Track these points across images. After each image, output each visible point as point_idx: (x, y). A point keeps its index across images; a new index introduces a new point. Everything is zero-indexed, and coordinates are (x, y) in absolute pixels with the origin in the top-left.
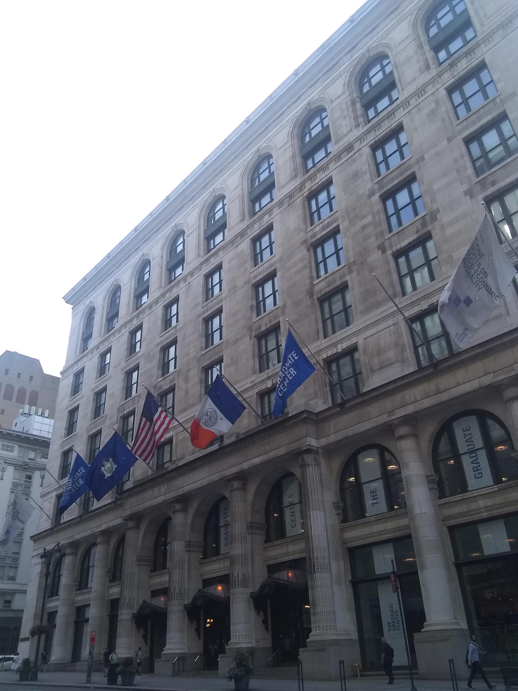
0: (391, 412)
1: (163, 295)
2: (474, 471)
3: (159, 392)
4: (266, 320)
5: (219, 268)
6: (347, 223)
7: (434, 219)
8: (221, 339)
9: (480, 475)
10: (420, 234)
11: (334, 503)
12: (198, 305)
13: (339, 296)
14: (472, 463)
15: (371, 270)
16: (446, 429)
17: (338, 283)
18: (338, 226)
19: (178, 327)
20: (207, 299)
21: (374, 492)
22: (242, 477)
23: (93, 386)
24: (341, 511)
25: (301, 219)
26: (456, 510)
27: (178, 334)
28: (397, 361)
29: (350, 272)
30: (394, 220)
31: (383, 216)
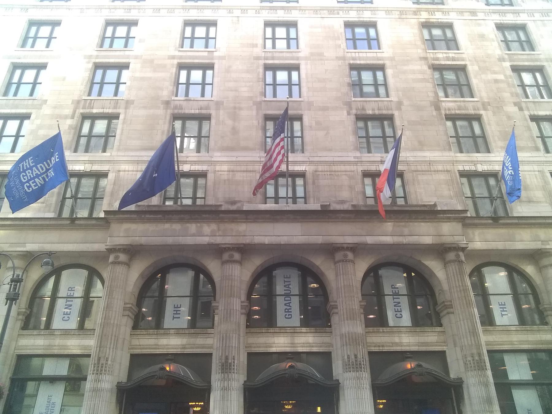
2: (285, 312)
9: (290, 316)
14: (285, 305)
21: (177, 309)
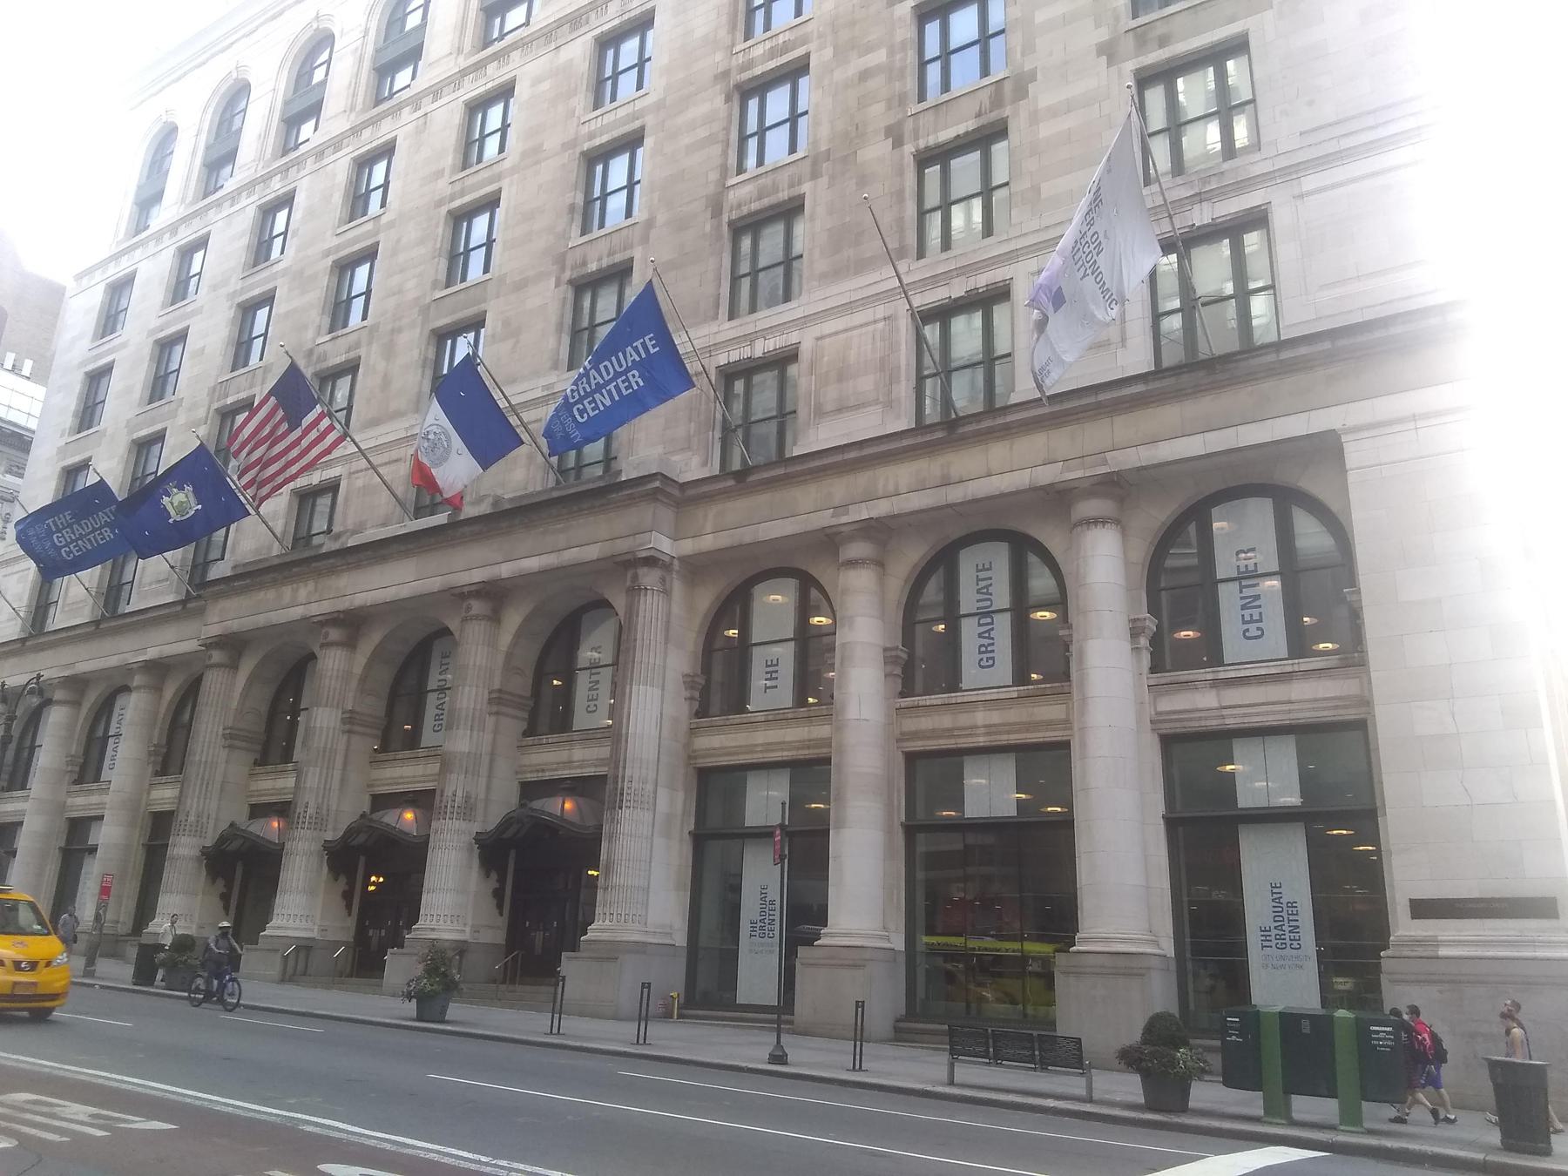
0: (842, 508)
1: (355, 131)
3: (318, 367)
4: (603, 247)
5: (505, 92)
6: (828, 52)
7: (1021, 92)
8: (486, 270)
10: (983, 121)
11: (687, 675)
12: (439, 174)
13: (779, 228)
14: (980, 635)
15: (863, 181)
16: (944, 561)
17: (783, 195)
18: (808, 55)
19: (384, 219)
20: (465, 165)
21: (772, 667)
22: (495, 594)
23: (155, 323)
24: (697, 694)
25: (724, 19)
26: (925, 723)
27: (381, 237)
28: (876, 402)
29: (815, 175)
30: (934, 72)
31: (911, 57)
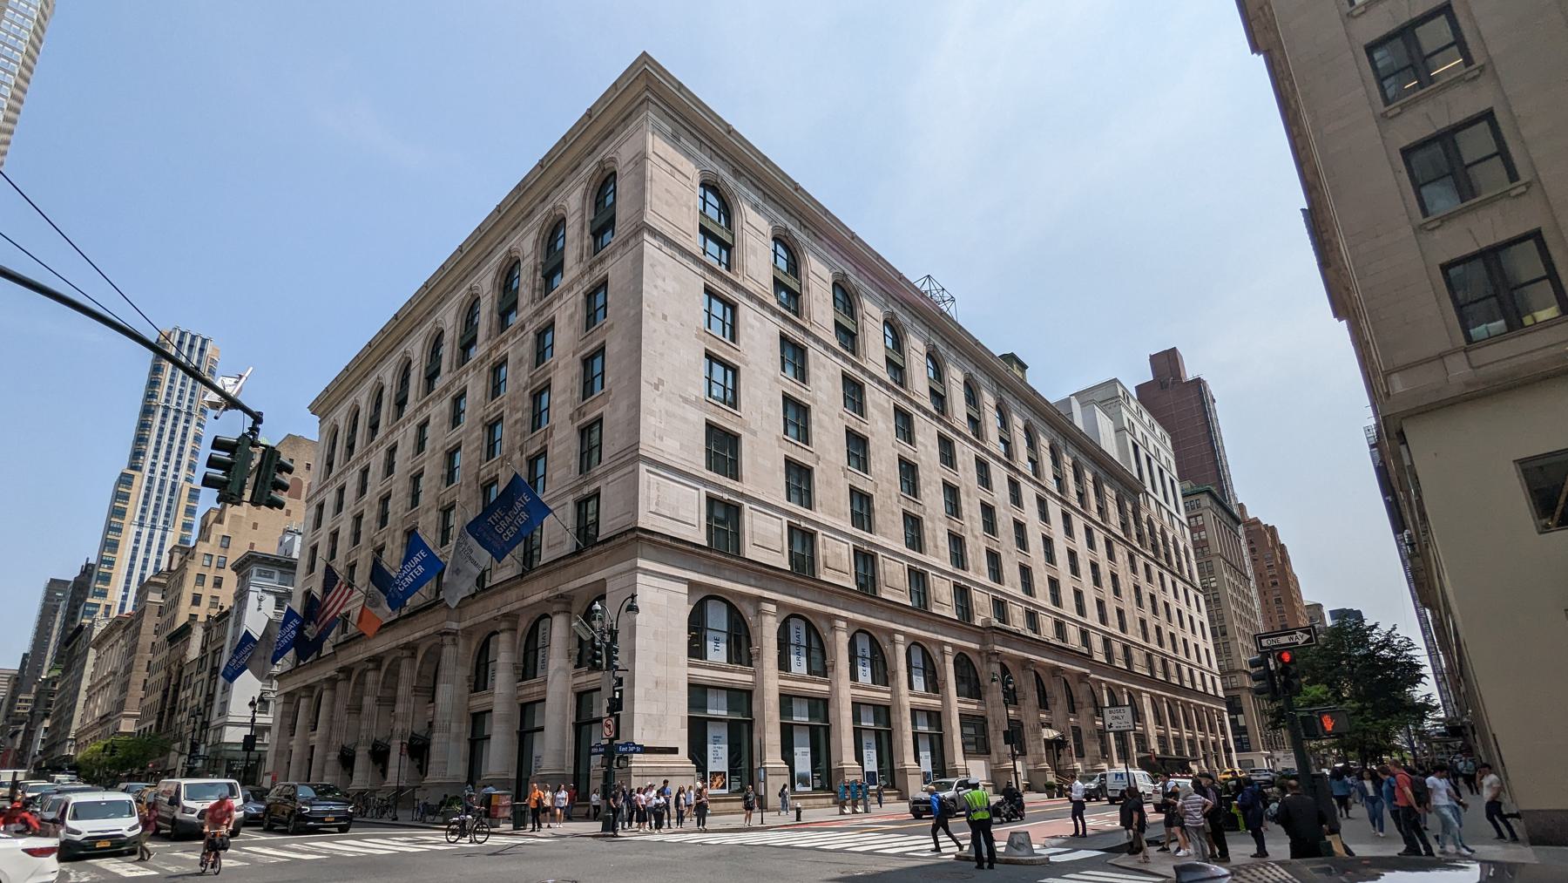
31: (528, 415)
